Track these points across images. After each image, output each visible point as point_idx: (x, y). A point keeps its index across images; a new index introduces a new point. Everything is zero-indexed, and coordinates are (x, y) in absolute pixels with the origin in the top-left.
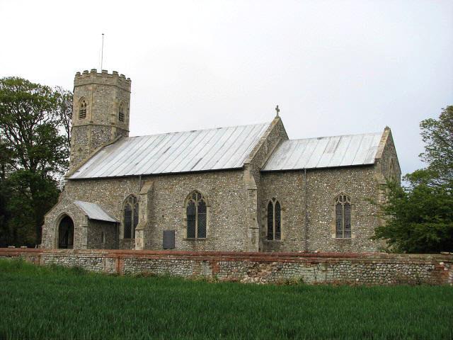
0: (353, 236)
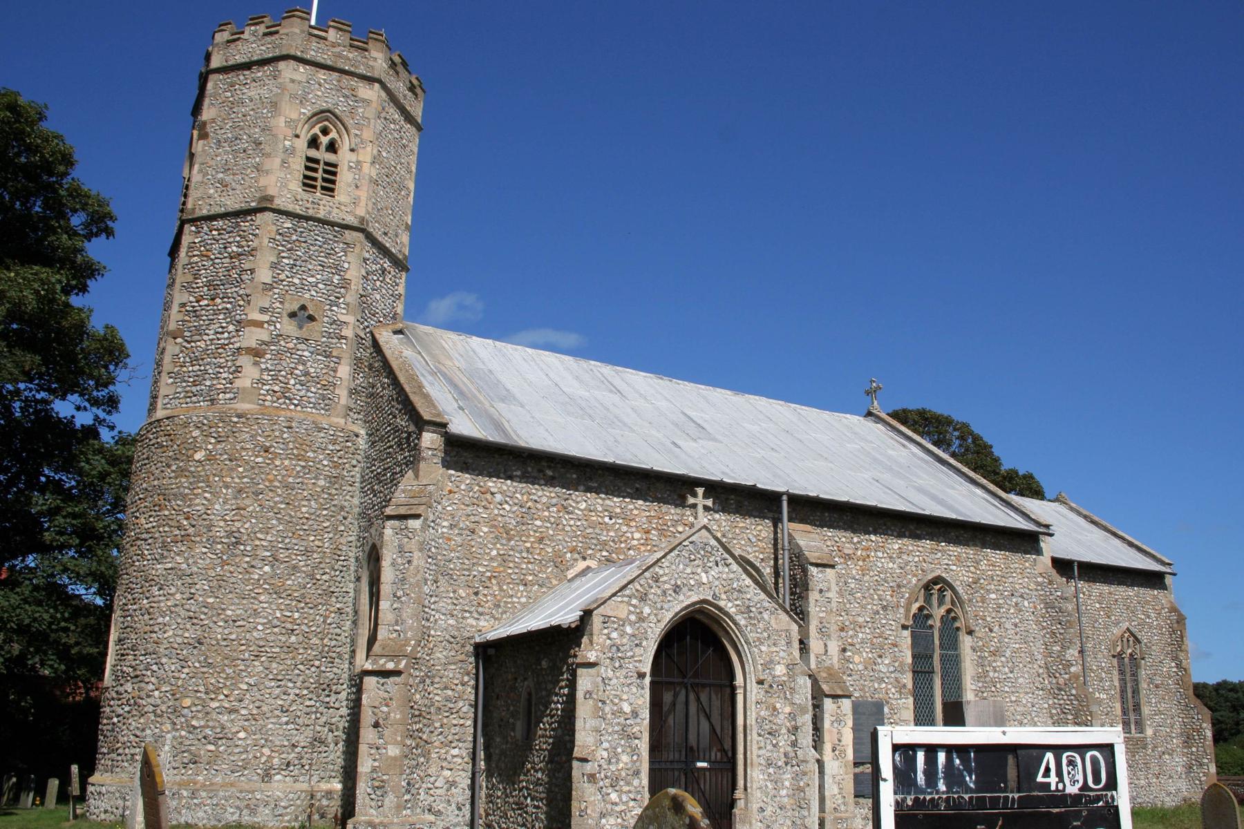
0: (1149, 732)
